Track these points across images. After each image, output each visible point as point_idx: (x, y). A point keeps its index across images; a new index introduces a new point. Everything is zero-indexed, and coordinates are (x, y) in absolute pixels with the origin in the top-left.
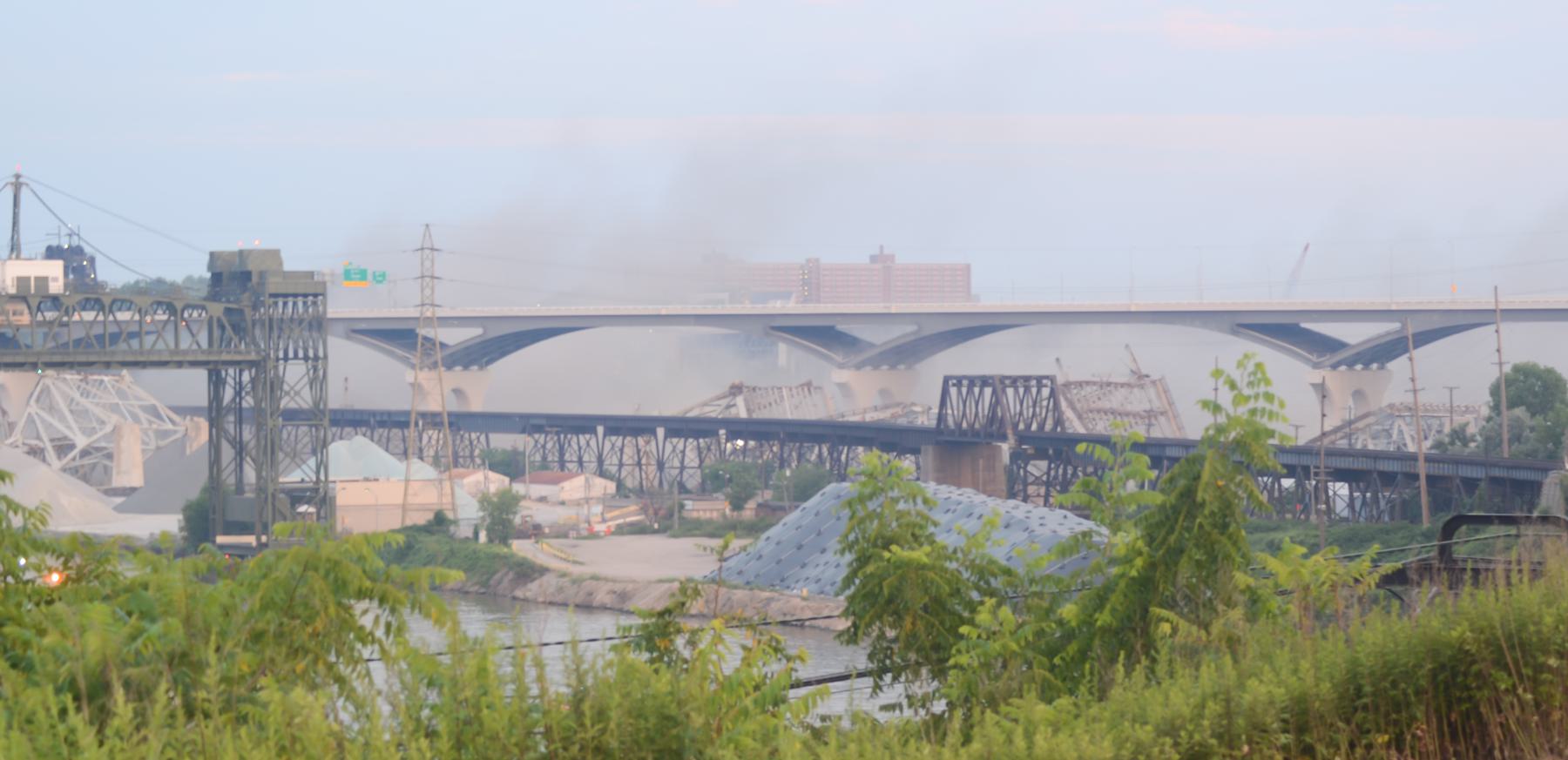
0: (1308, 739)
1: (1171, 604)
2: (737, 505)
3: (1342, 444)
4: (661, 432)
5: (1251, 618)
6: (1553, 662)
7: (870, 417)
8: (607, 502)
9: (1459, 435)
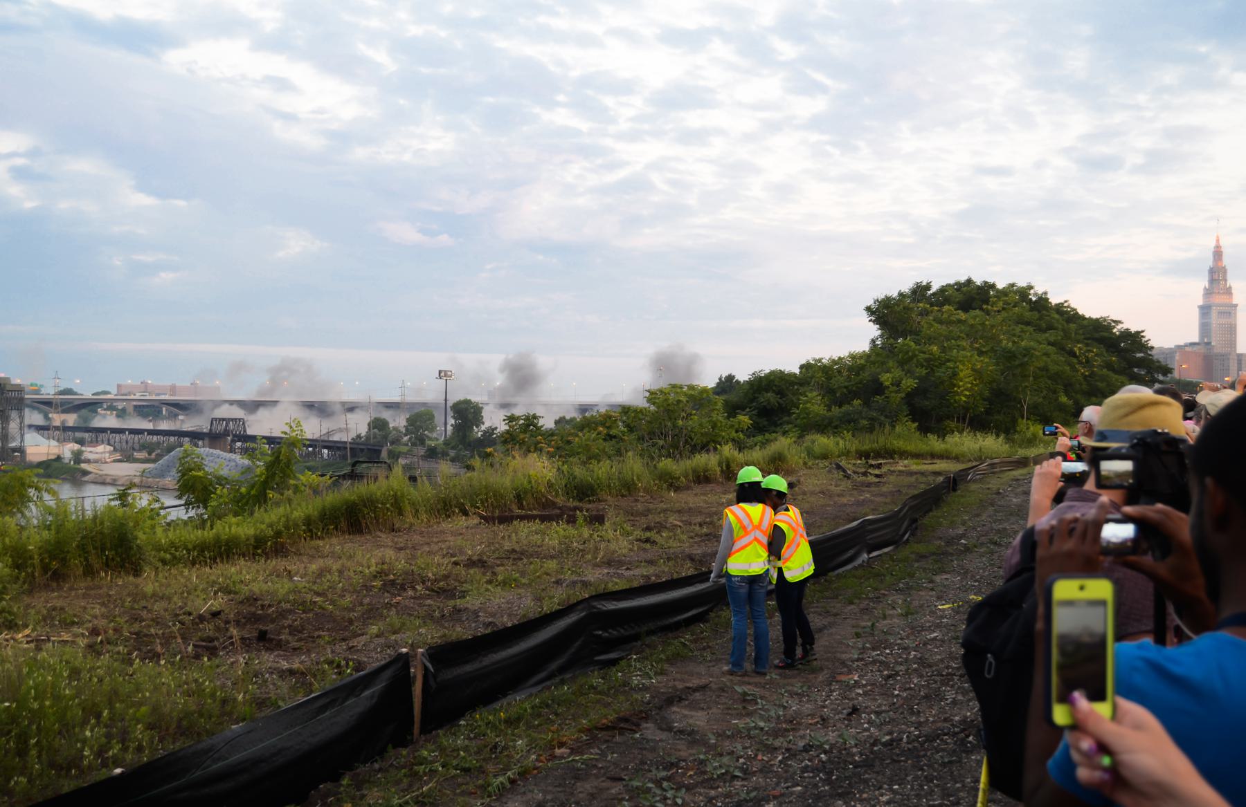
0: (311, 527)
1: (272, 489)
2: (150, 454)
3: (326, 439)
4: (127, 433)
5: (295, 493)
6: (380, 506)
7: (190, 429)
8: (111, 453)
9: (359, 436)
